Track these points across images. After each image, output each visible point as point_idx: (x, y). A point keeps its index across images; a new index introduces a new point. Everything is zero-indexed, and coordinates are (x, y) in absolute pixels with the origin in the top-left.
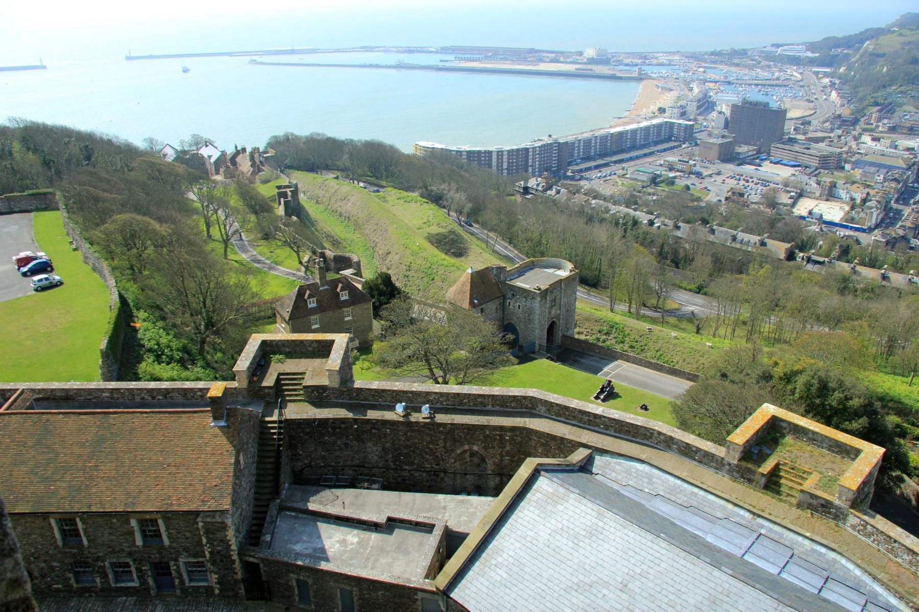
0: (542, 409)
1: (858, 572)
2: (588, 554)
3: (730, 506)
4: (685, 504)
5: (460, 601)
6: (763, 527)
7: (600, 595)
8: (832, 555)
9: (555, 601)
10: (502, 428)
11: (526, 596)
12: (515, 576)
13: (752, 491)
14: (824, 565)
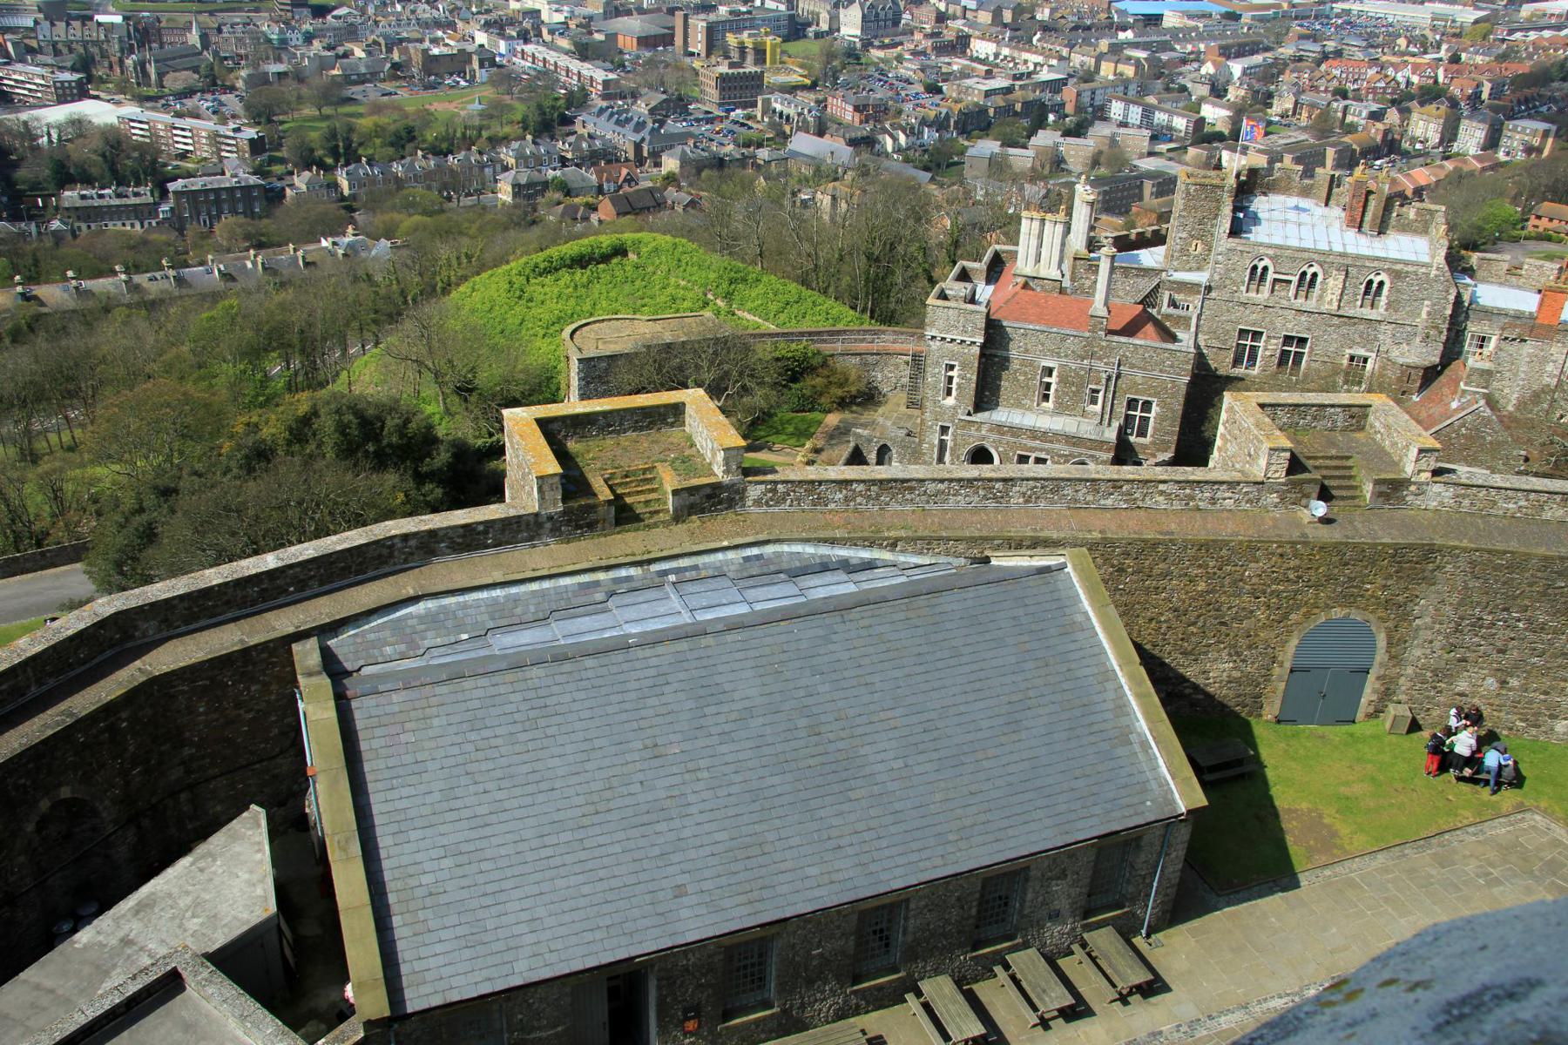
0: (150, 627)
1: (809, 549)
2: (556, 751)
3: (601, 576)
4: (541, 616)
5: (436, 1001)
6: (665, 573)
7: (636, 788)
8: (769, 550)
9: (583, 855)
10: (108, 709)
11: (535, 890)
12: (481, 879)
13: (602, 539)
14: (772, 568)
